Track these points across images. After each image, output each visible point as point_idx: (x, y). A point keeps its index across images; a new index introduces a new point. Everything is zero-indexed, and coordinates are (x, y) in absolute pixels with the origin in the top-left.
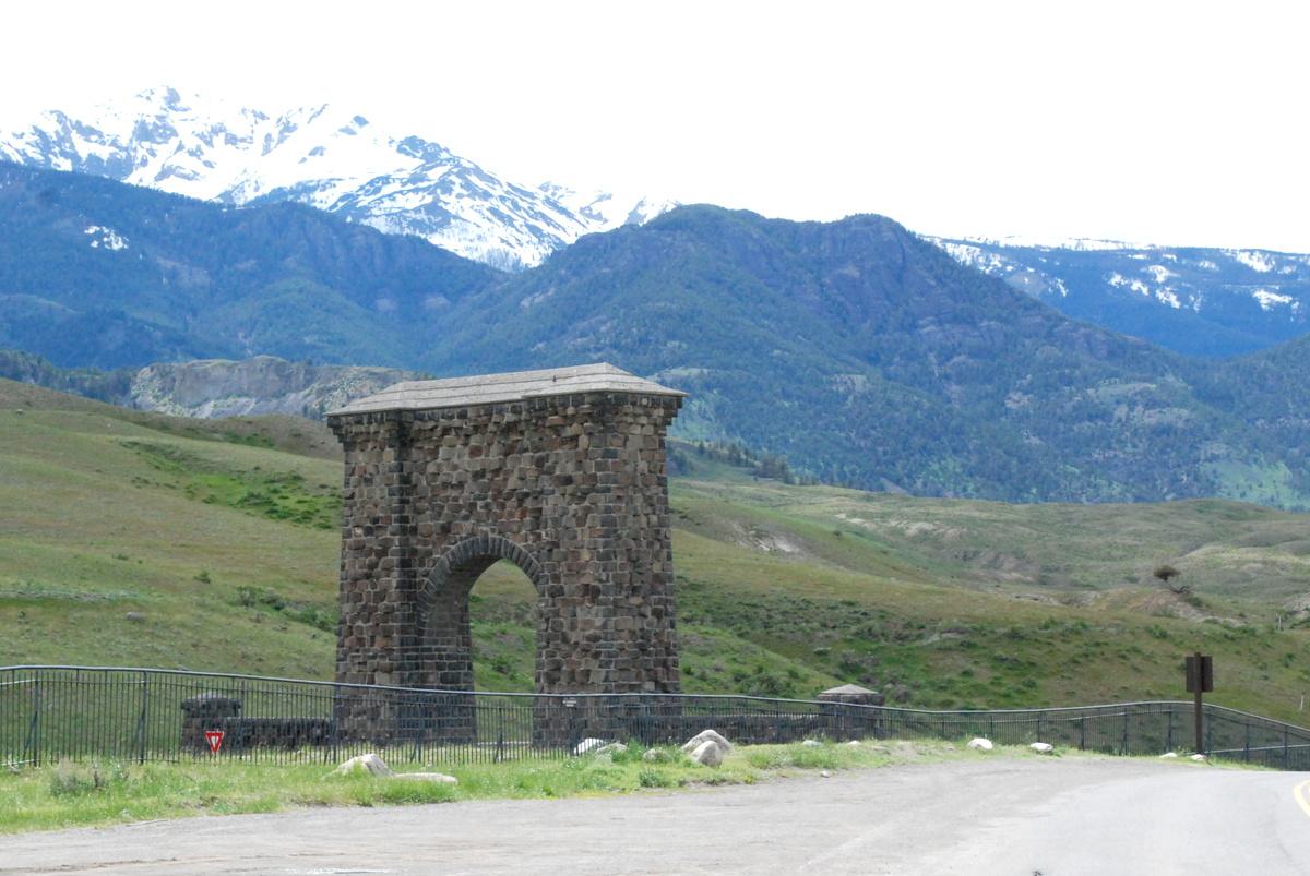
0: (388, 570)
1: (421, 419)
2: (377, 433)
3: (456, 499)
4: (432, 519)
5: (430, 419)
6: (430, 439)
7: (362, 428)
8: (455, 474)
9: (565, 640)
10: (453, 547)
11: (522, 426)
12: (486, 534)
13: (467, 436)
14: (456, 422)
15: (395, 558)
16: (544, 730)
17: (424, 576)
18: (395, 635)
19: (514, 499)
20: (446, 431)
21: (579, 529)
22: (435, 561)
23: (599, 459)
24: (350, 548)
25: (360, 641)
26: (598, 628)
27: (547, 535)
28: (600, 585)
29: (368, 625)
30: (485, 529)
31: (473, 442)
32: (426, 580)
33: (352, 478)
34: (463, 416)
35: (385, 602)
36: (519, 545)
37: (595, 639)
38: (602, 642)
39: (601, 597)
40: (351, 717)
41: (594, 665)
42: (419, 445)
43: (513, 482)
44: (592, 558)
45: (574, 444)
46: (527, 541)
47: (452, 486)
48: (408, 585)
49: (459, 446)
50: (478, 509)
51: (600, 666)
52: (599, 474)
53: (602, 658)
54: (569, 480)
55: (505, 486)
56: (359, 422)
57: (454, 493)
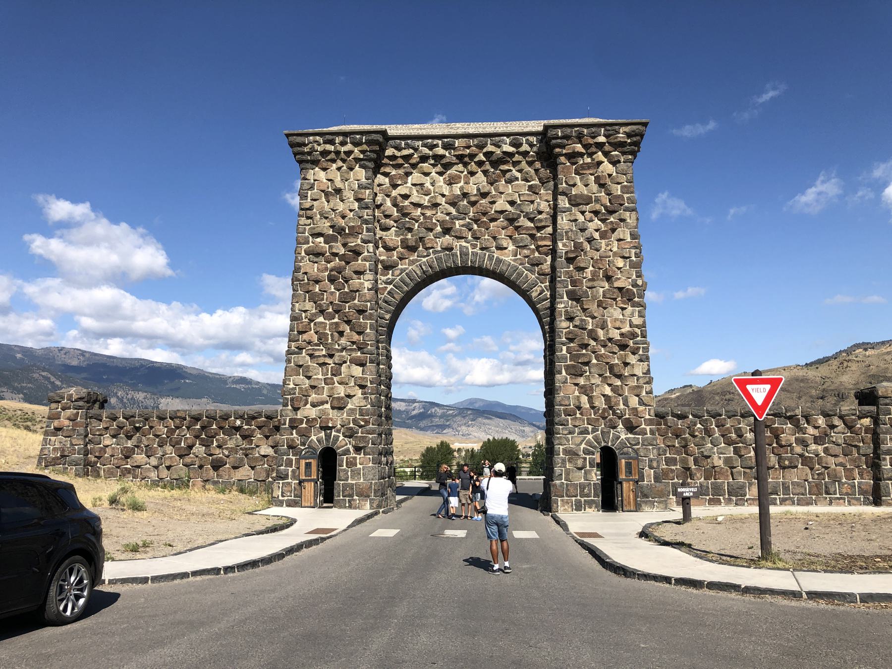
0: (359, 273)
1: (399, 149)
2: (349, 153)
3: (431, 218)
4: (397, 235)
5: (408, 146)
6: (398, 166)
7: (331, 148)
8: (427, 198)
9: (593, 335)
10: (424, 260)
11: (517, 158)
12: (467, 248)
13: (447, 166)
14: (440, 151)
15: (367, 264)
16: (569, 418)
17: (386, 283)
18: (368, 331)
19: (502, 219)
20: (424, 159)
21: (603, 241)
22: (402, 271)
23: (625, 183)
24: (307, 253)
25: (322, 337)
26: (637, 326)
27: (564, 245)
28: (635, 290)
29: (333, 321)
30: (464, 244)
31: (452, 171)
32: (390, 287)
33: (309, 192)
34: (446, 147)
35: (356, 301)
36: (506, 259)
37: (633, 335)
38: (639, 338)
39: (636, 299)
40: (308, 406)
41: (632, 359)
42: (387, 170)
43: (501, 204)
44: (625, 265)
45: (595, 170)
46: (516, 256)
47: (427, 207)
48: (375, 289)
49: (433, 174)
50: (457, 226)
51: (641, 360)
52: (626, 196)
53: (641, 352)
54: (588, 200)
55: (492, 208)
56: (332, 142)
57: (429, 213)
